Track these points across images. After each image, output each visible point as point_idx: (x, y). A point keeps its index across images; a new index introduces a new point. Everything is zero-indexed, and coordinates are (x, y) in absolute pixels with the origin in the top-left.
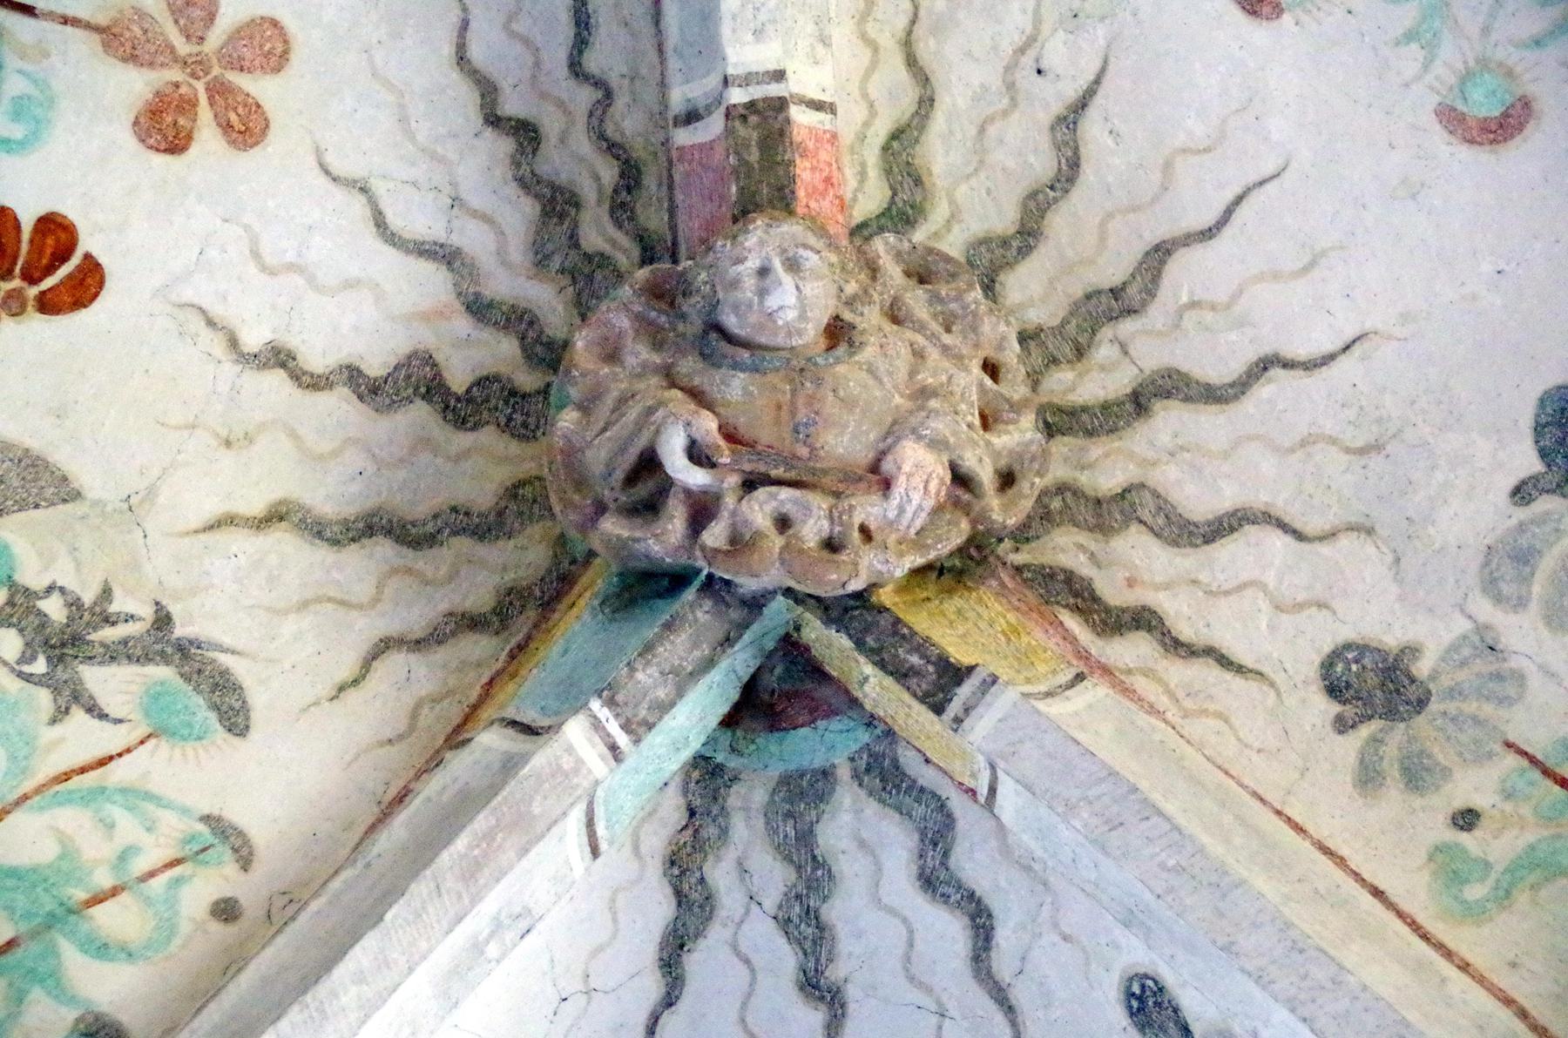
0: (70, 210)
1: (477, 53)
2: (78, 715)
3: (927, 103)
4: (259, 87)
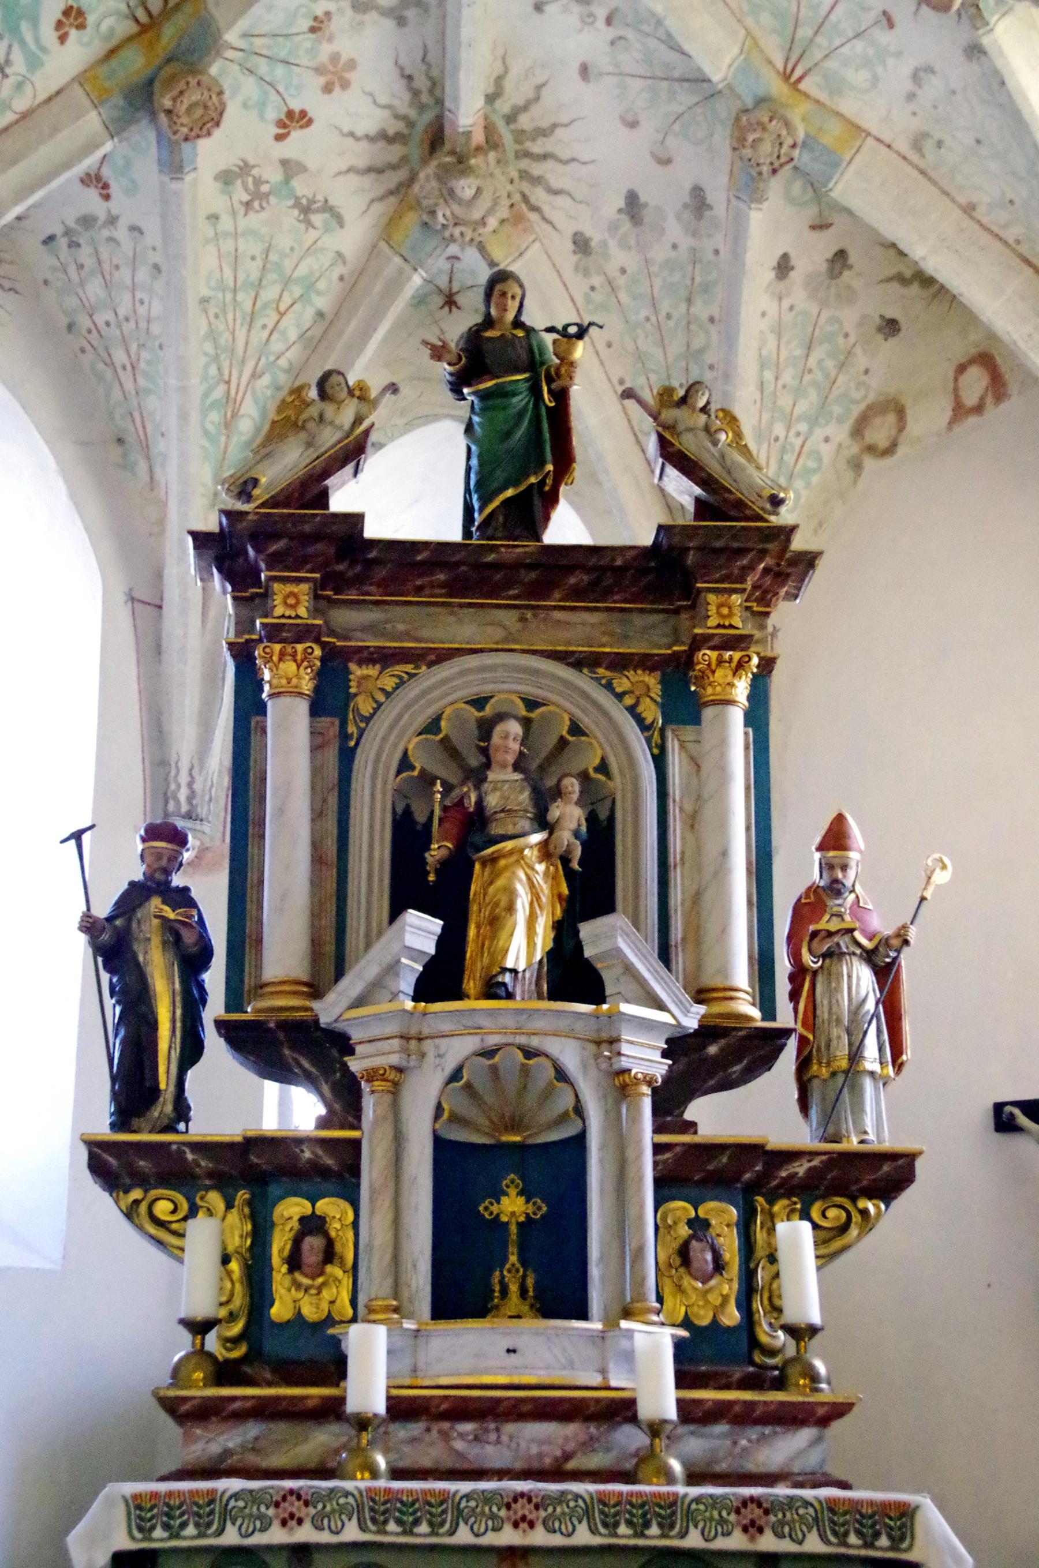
0: (307, 108)
1: (400, 62)
2: (310, 229)
3: (506, 72)
4: (348, 75)
